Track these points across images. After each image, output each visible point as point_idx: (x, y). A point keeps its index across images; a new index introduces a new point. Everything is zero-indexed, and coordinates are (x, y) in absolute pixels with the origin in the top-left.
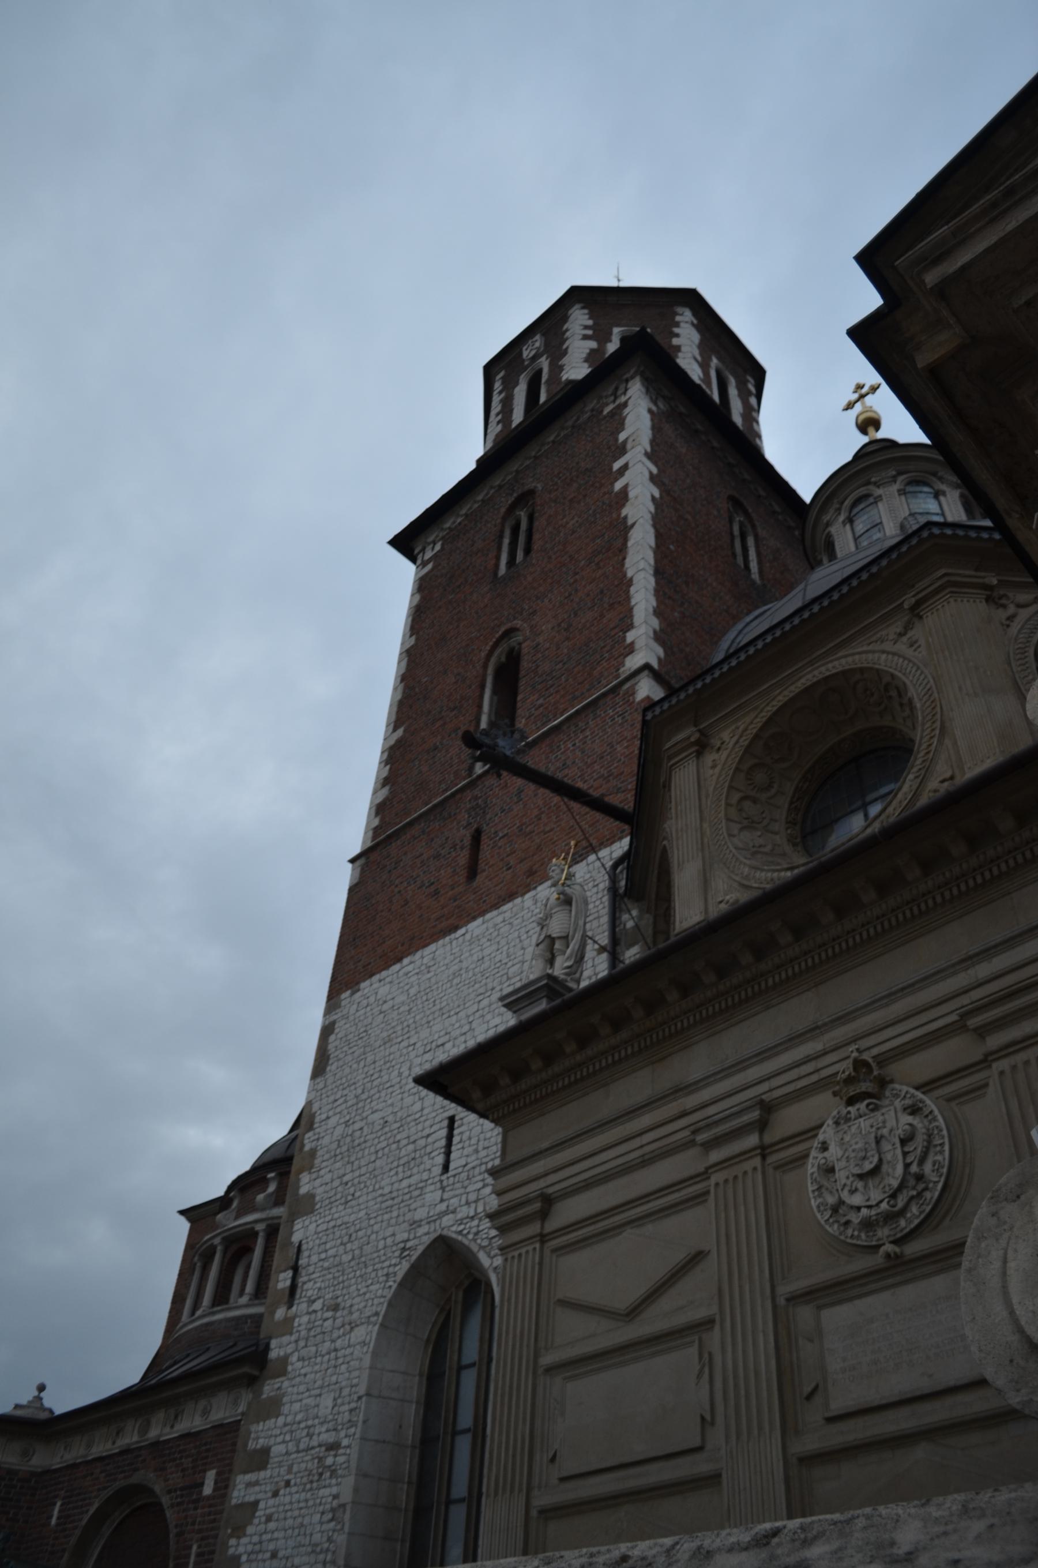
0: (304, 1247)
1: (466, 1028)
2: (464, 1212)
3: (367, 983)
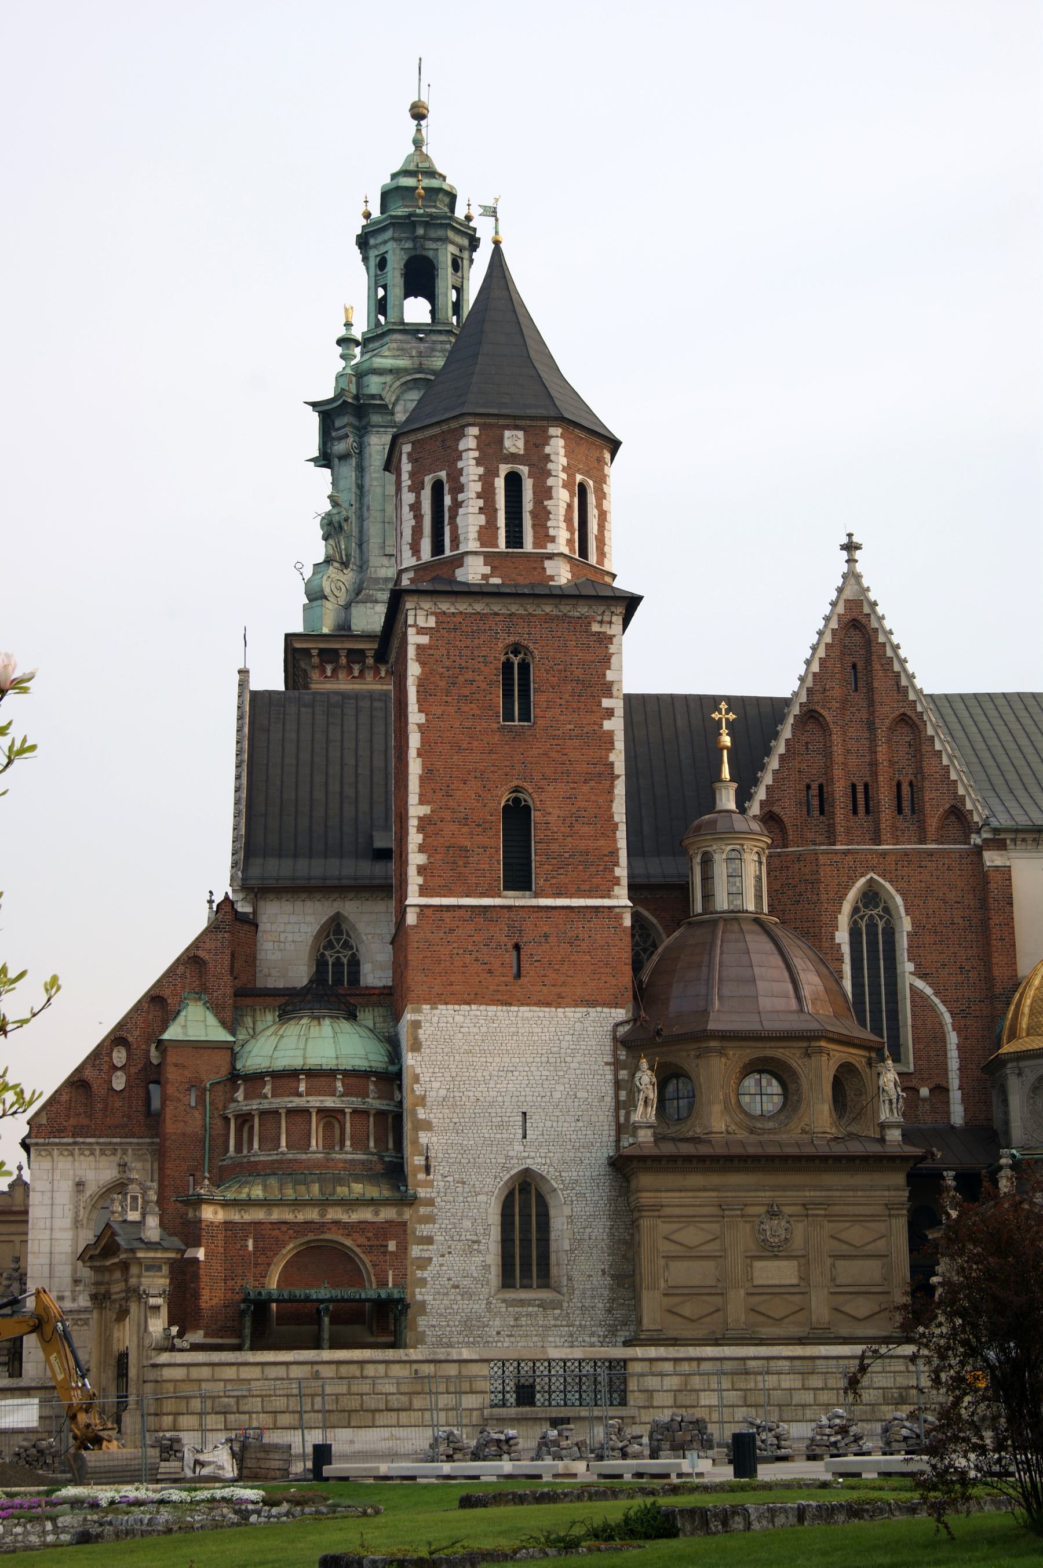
3: (444, 1007)
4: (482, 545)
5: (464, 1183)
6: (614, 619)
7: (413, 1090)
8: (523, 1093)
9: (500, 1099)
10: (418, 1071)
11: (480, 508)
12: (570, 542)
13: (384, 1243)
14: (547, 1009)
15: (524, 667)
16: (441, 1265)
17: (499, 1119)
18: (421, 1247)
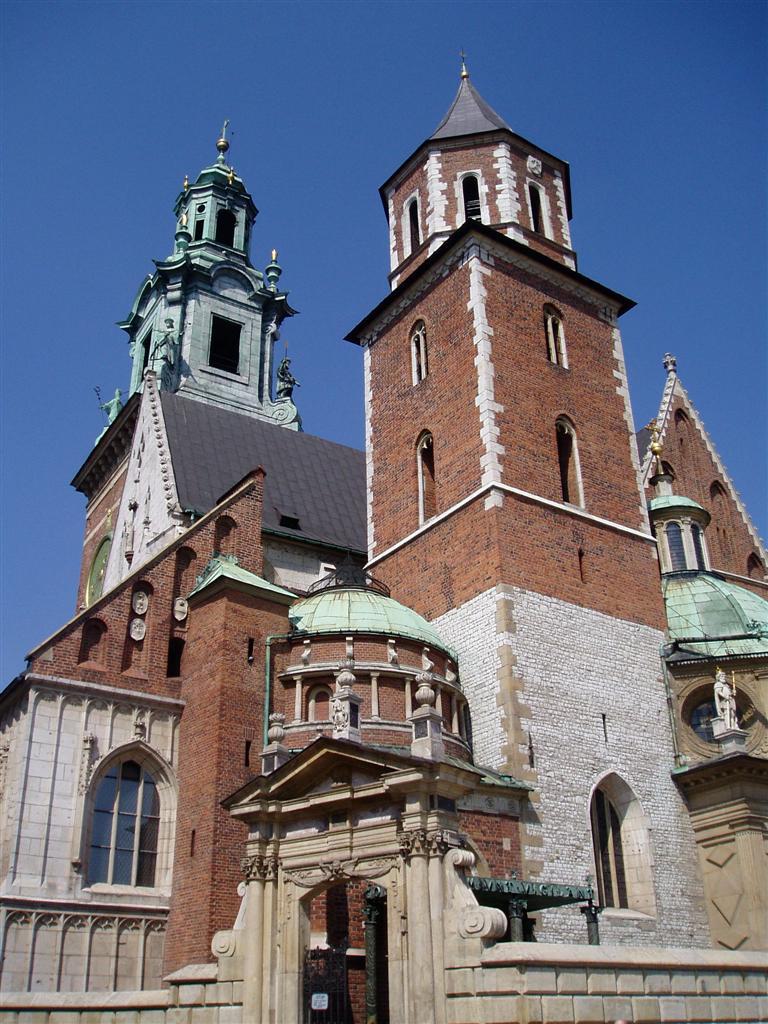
9: (584, 696)
13: (499, 840)
14: (609, 617)
16: (552, 872)
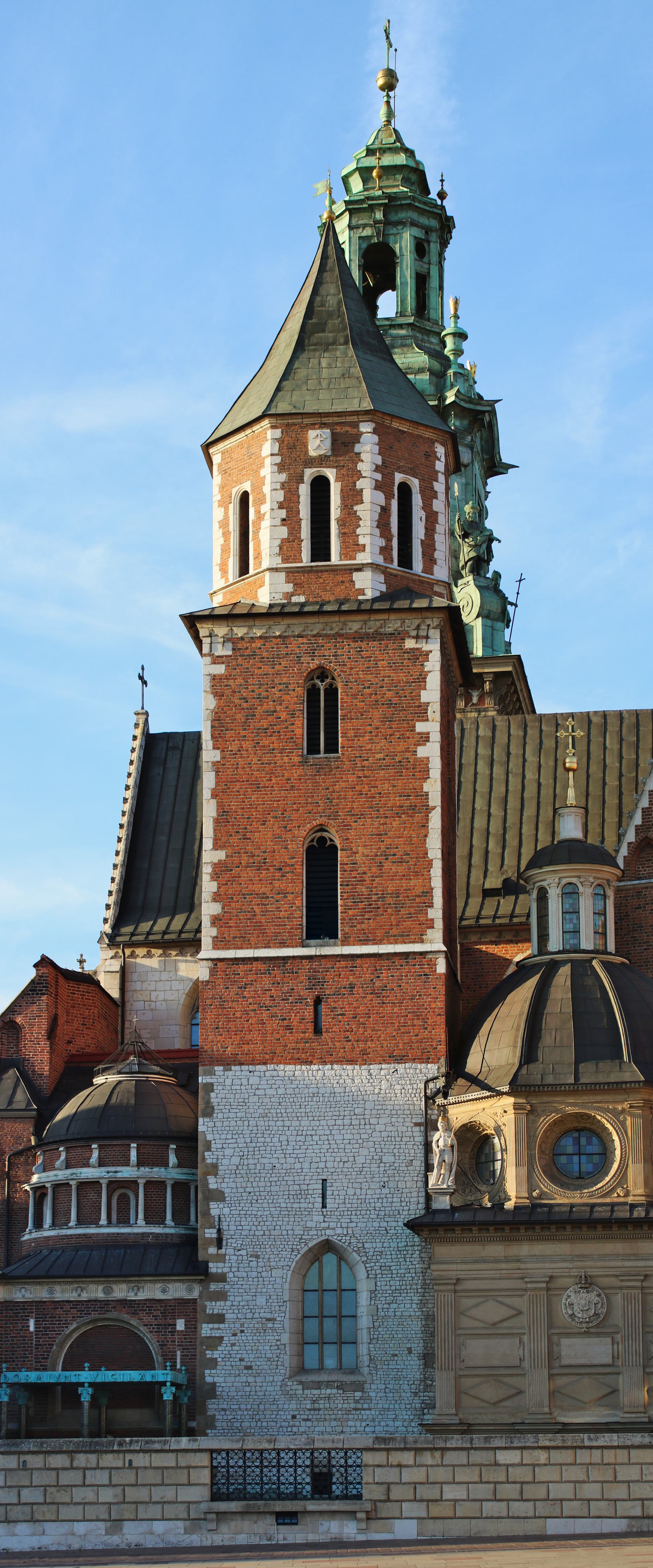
0: (223, 1219)
1: (328, 1132)
2: (339, 1231)
3: (237, 1068)
4: (285, 560)
5: (257, 1257)
6: (432, 632)
7: (204, 1159)
8: (323, 1159)
10: (209, 1137)
11: (283, 520)
12: (385, 551)
13: (170, 1322)
15: (332, 693)
16: (233, 1345)
17: (298, 1187)
18: (211, 1326)
